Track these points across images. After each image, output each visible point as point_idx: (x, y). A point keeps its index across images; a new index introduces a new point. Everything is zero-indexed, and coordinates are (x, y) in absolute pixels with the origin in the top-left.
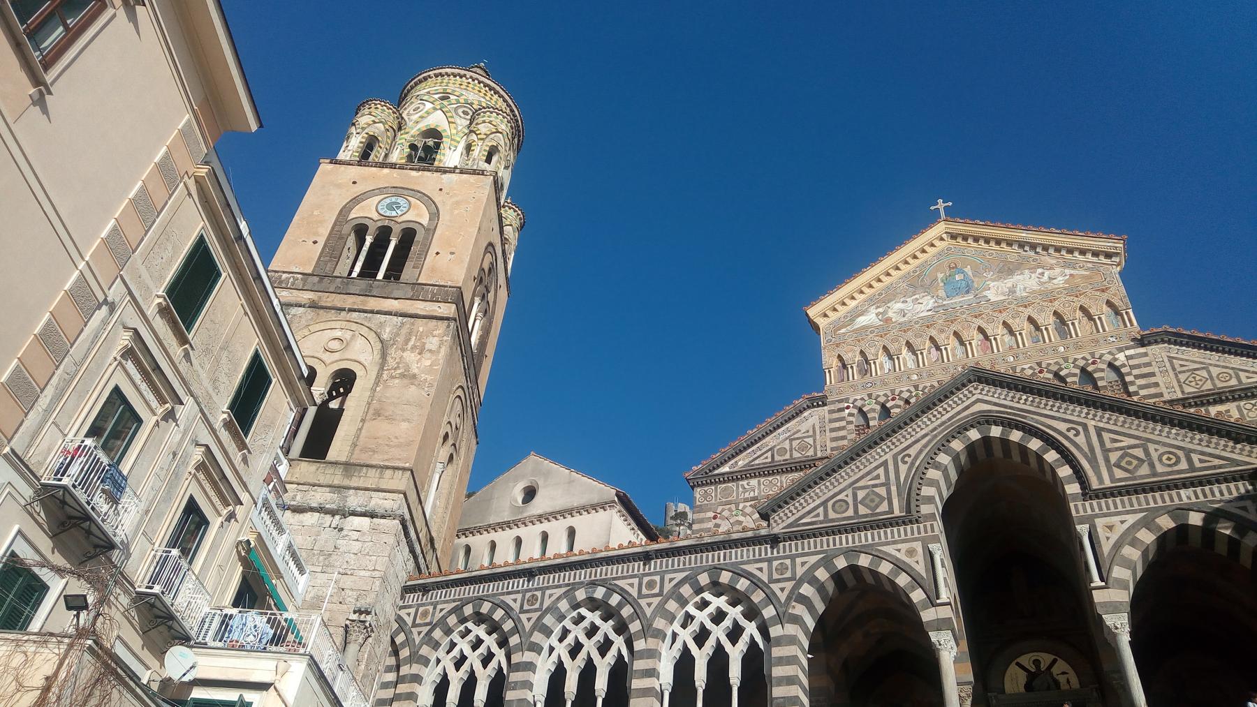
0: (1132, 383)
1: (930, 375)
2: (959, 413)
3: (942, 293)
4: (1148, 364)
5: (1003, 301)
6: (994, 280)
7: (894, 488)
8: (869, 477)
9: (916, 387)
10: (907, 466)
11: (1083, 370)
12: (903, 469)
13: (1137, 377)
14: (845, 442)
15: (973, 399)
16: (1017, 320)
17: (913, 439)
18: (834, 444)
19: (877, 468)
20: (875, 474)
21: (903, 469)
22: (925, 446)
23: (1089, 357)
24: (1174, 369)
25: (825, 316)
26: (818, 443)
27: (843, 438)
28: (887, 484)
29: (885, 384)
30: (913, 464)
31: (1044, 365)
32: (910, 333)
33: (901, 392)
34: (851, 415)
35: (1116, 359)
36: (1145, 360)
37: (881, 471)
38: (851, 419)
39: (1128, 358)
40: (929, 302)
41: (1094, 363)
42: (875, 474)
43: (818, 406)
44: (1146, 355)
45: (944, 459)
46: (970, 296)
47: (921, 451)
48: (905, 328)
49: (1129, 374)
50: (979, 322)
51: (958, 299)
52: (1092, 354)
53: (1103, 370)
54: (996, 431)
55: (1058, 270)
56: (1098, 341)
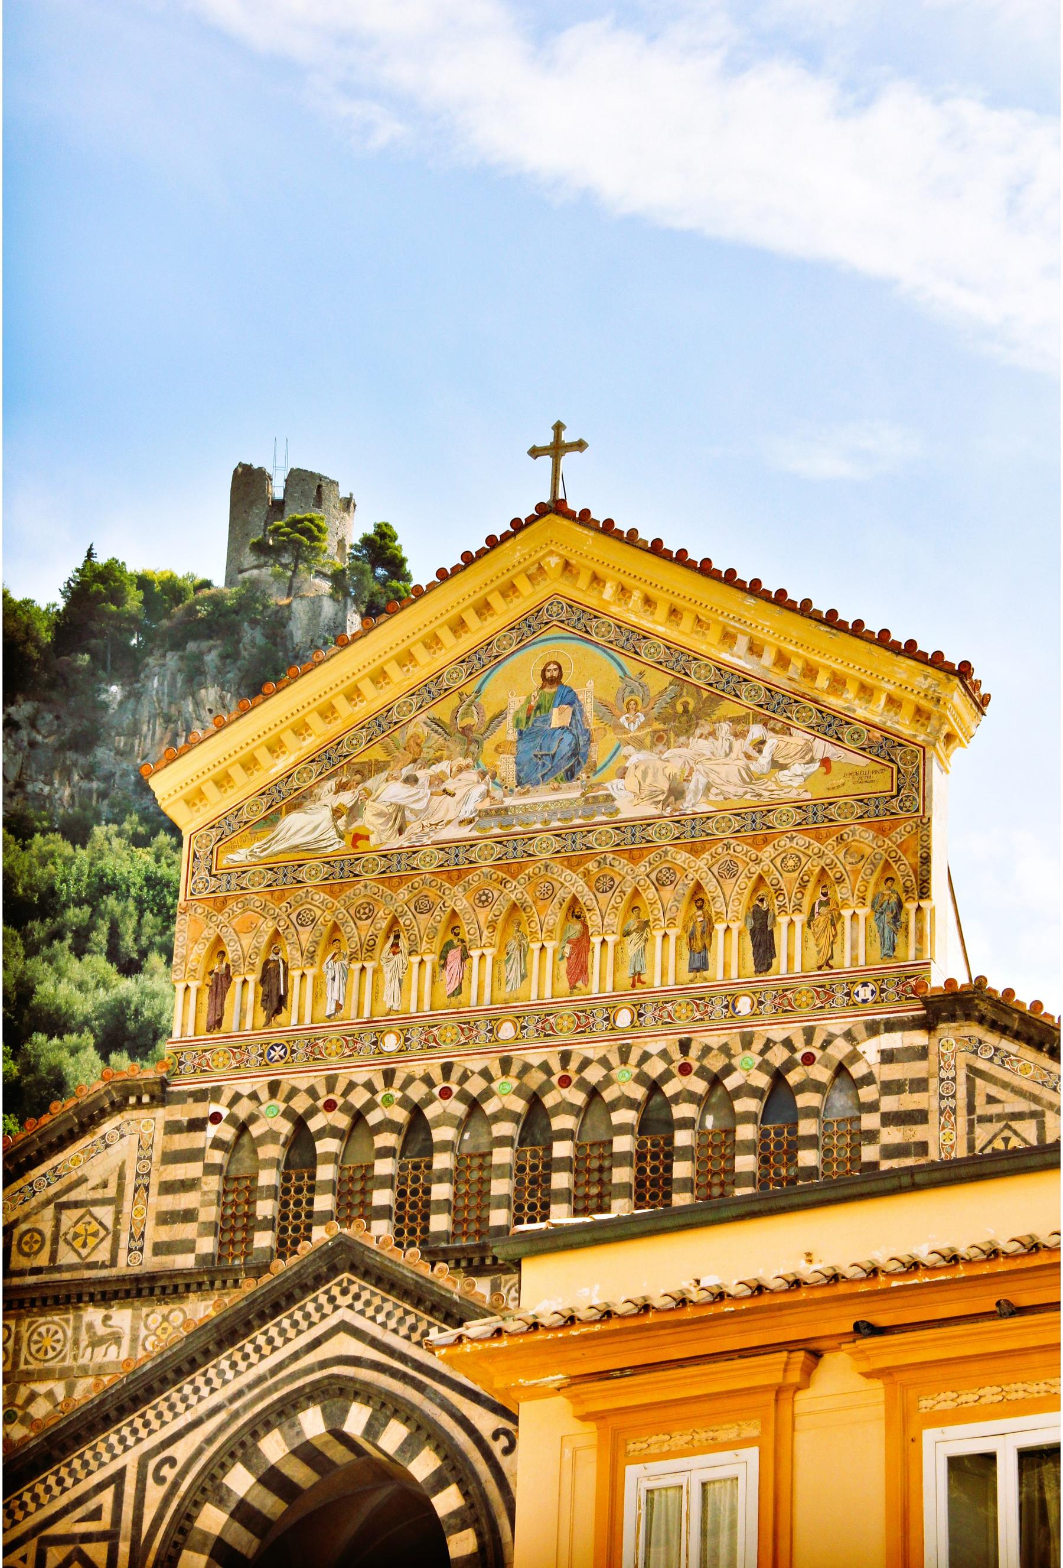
0: (871, 1136)
1: (430, 1044)
2: (295, 1356)
3: (507, 767)
4: (920, 1085)
5: (648, 822)
6: (639, 744)
7: (124, 1548)
8: (80, 1512)
9: (389, 1077)
10: (162, 1490)
11: (778, 1076)
12: (155, 1494)
13: (891, 1119)
14: (186, 1231)
15: (333, 1320)
16: (667, 893)
17: (188, 1417)
18: (165, 1234)
19: (100, 1487)
20: (91, 1505)
21: (155, 1494)
22: (209, 1441)
23: (799, 1041)
24: (971, 1108)
25: (200, 793)
26: (125, 1219)
27: (188, 1216)
28: (111, 1537)
29: (314, 1054)
30: (175, 1485)
31: (694, 1052)
32: (403, 894)
33: (351, 1086)
34: (218, 1144)
35: (855, 1057)
36: (916, 1069)
37: (106, 1497)
38: (217, 1157)
39: (888, 1057)
40: (470, 793)
41: (809, 1059)
42: (91, 1505)
43: (139, 1104)
44: (922, 1053)
45: (240, 1481)
46: (571, 792)
47: (199, 1452)
48: (396, 869)
49: (873, 1107)
50: (573, 883)
51: (543, 796)
52: (809, 1034)
53: (817, 1087)
54: (357, 1419)
55: (799, 738)
56: (830, 995)
